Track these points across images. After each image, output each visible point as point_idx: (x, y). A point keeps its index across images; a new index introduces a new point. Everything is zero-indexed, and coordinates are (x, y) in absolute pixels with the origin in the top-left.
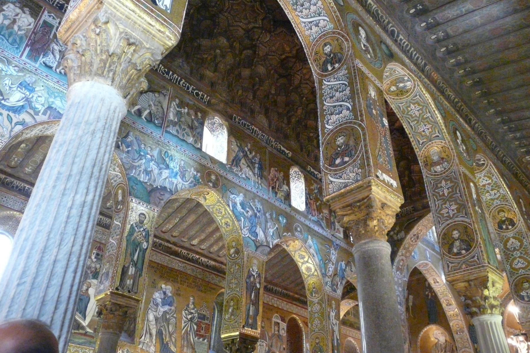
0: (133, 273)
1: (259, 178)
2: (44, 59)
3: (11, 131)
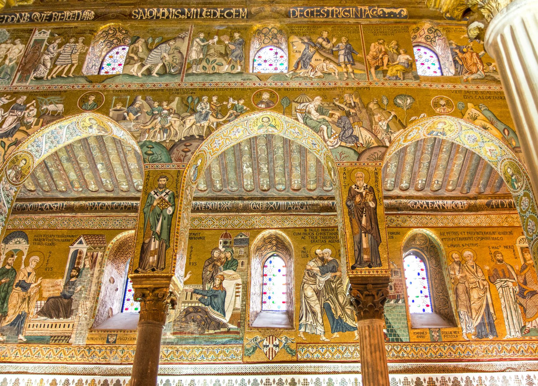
0: (157, 247)
1: (349, 66)
2: (35, 75)
3: (5, 154)
